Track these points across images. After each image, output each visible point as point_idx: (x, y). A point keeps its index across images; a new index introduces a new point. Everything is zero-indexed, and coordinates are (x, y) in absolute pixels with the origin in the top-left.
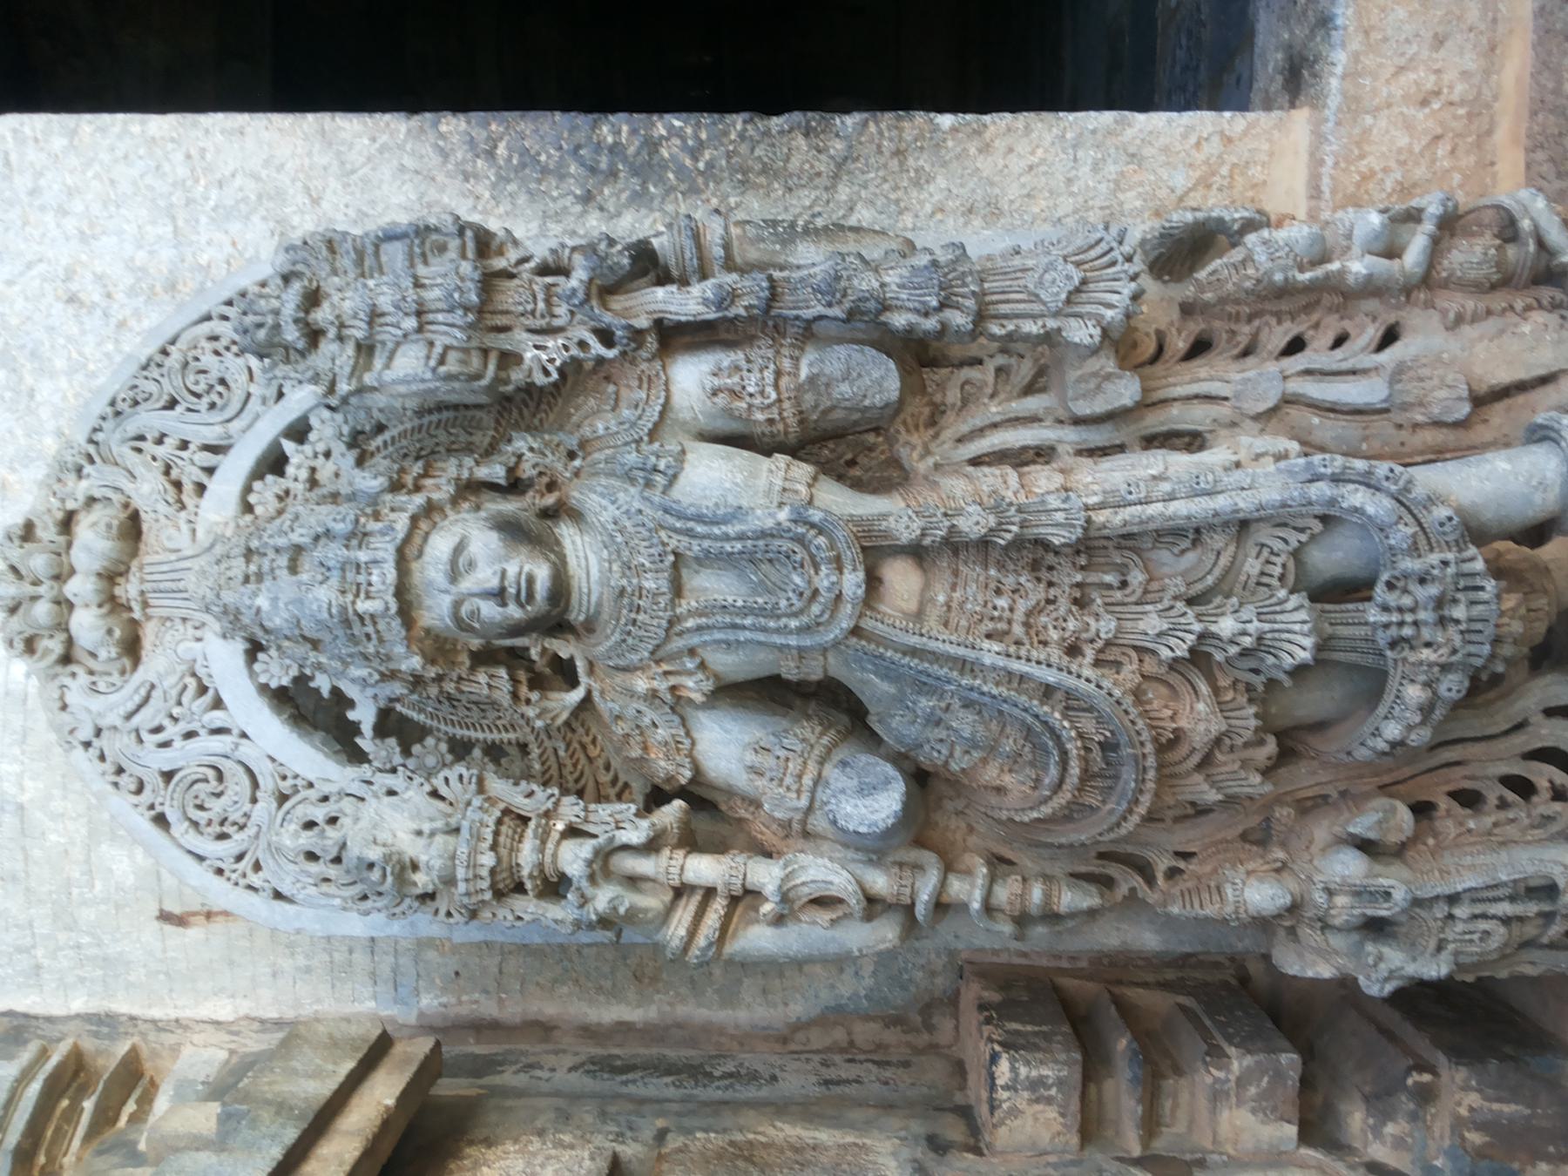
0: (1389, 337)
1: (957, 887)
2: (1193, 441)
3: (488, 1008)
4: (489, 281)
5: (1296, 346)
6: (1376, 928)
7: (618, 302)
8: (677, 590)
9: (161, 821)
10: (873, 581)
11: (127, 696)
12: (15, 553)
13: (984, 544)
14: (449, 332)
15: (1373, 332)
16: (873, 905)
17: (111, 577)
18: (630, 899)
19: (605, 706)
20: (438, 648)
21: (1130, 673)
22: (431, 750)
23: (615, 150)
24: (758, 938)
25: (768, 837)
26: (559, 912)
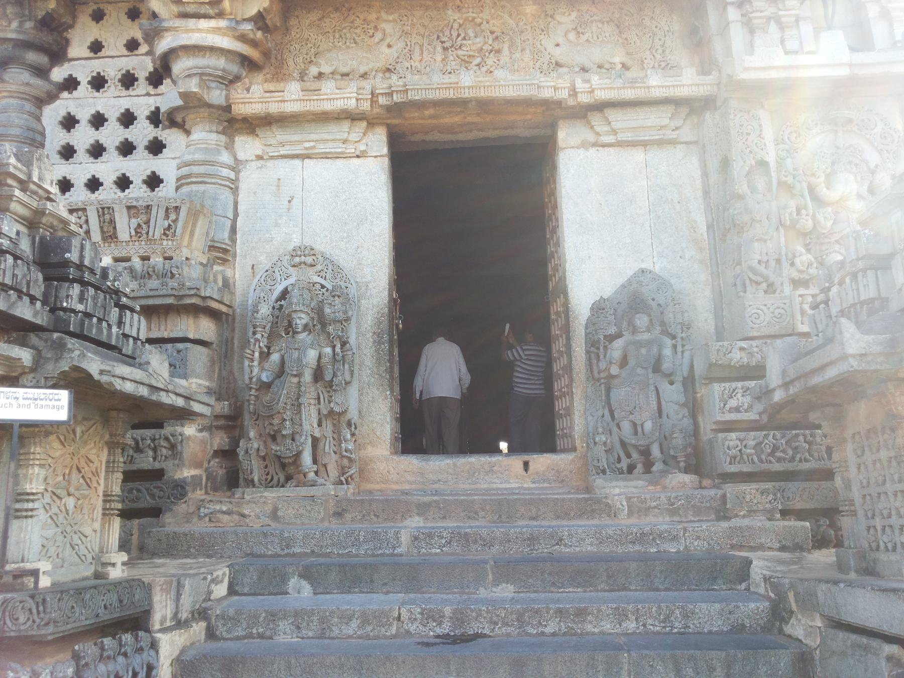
0: (335, 453)
1: (253, 391)
2: (320, 425)
3: (237, 321)
4: (340, 322)
5: (334, 439)
6: (247, 452)
7: (338, 339)
8: (295, 349)
9: (267, 271)
10: (295, 376)
11: (287, 265)
12: (308, 248)
13: (300, 390)
14: (332, 316)
15: (336, 450)
16: (251, 379)
17: (304, 263)
18: (252, 344)
19: (282, 340)
20: (289, 315)
21: (282, 411)
22: (277, 313)
23: (383, 338)
24: (247, 363)
25: (262, 364)
26: (251, 334)
